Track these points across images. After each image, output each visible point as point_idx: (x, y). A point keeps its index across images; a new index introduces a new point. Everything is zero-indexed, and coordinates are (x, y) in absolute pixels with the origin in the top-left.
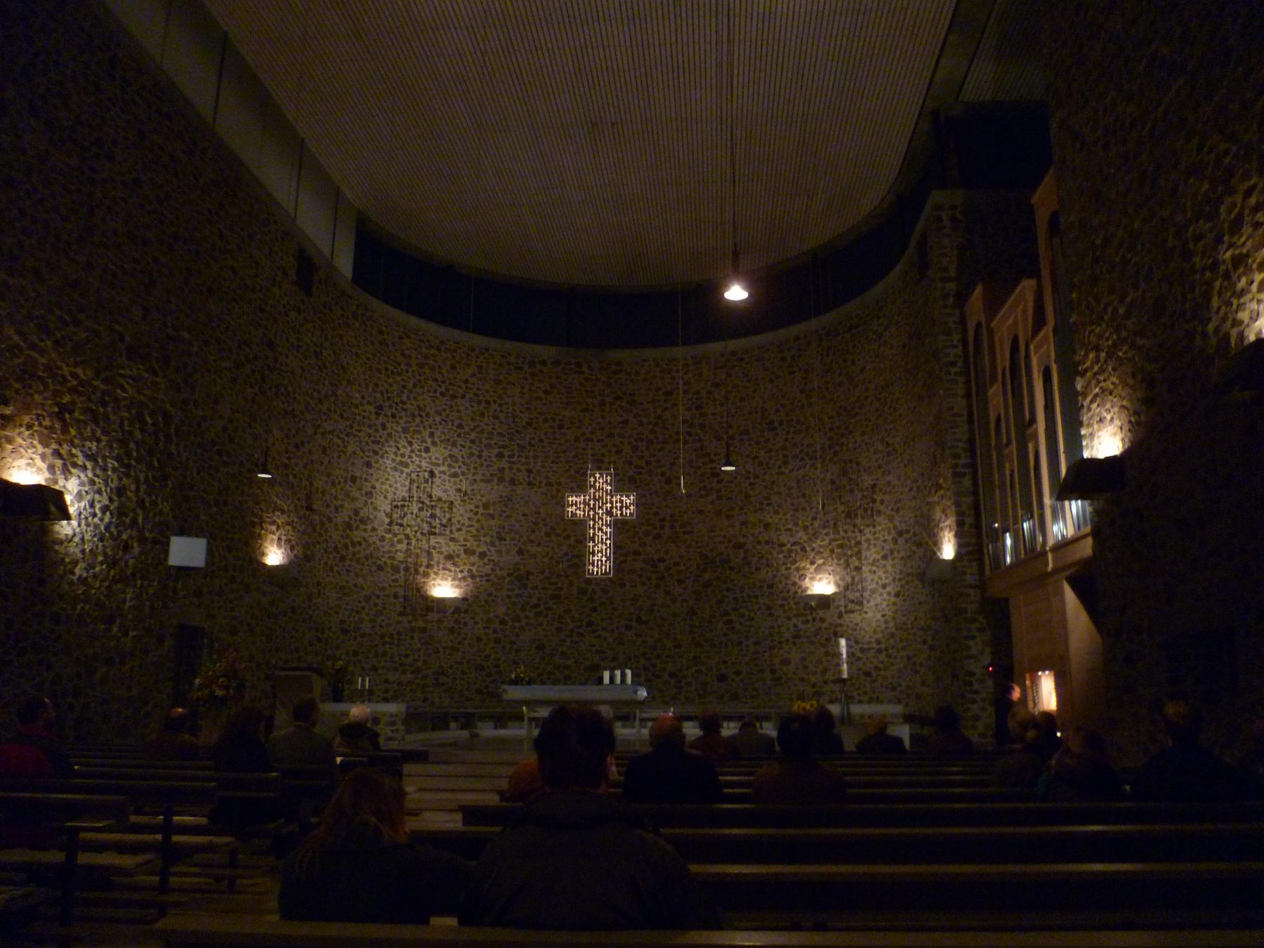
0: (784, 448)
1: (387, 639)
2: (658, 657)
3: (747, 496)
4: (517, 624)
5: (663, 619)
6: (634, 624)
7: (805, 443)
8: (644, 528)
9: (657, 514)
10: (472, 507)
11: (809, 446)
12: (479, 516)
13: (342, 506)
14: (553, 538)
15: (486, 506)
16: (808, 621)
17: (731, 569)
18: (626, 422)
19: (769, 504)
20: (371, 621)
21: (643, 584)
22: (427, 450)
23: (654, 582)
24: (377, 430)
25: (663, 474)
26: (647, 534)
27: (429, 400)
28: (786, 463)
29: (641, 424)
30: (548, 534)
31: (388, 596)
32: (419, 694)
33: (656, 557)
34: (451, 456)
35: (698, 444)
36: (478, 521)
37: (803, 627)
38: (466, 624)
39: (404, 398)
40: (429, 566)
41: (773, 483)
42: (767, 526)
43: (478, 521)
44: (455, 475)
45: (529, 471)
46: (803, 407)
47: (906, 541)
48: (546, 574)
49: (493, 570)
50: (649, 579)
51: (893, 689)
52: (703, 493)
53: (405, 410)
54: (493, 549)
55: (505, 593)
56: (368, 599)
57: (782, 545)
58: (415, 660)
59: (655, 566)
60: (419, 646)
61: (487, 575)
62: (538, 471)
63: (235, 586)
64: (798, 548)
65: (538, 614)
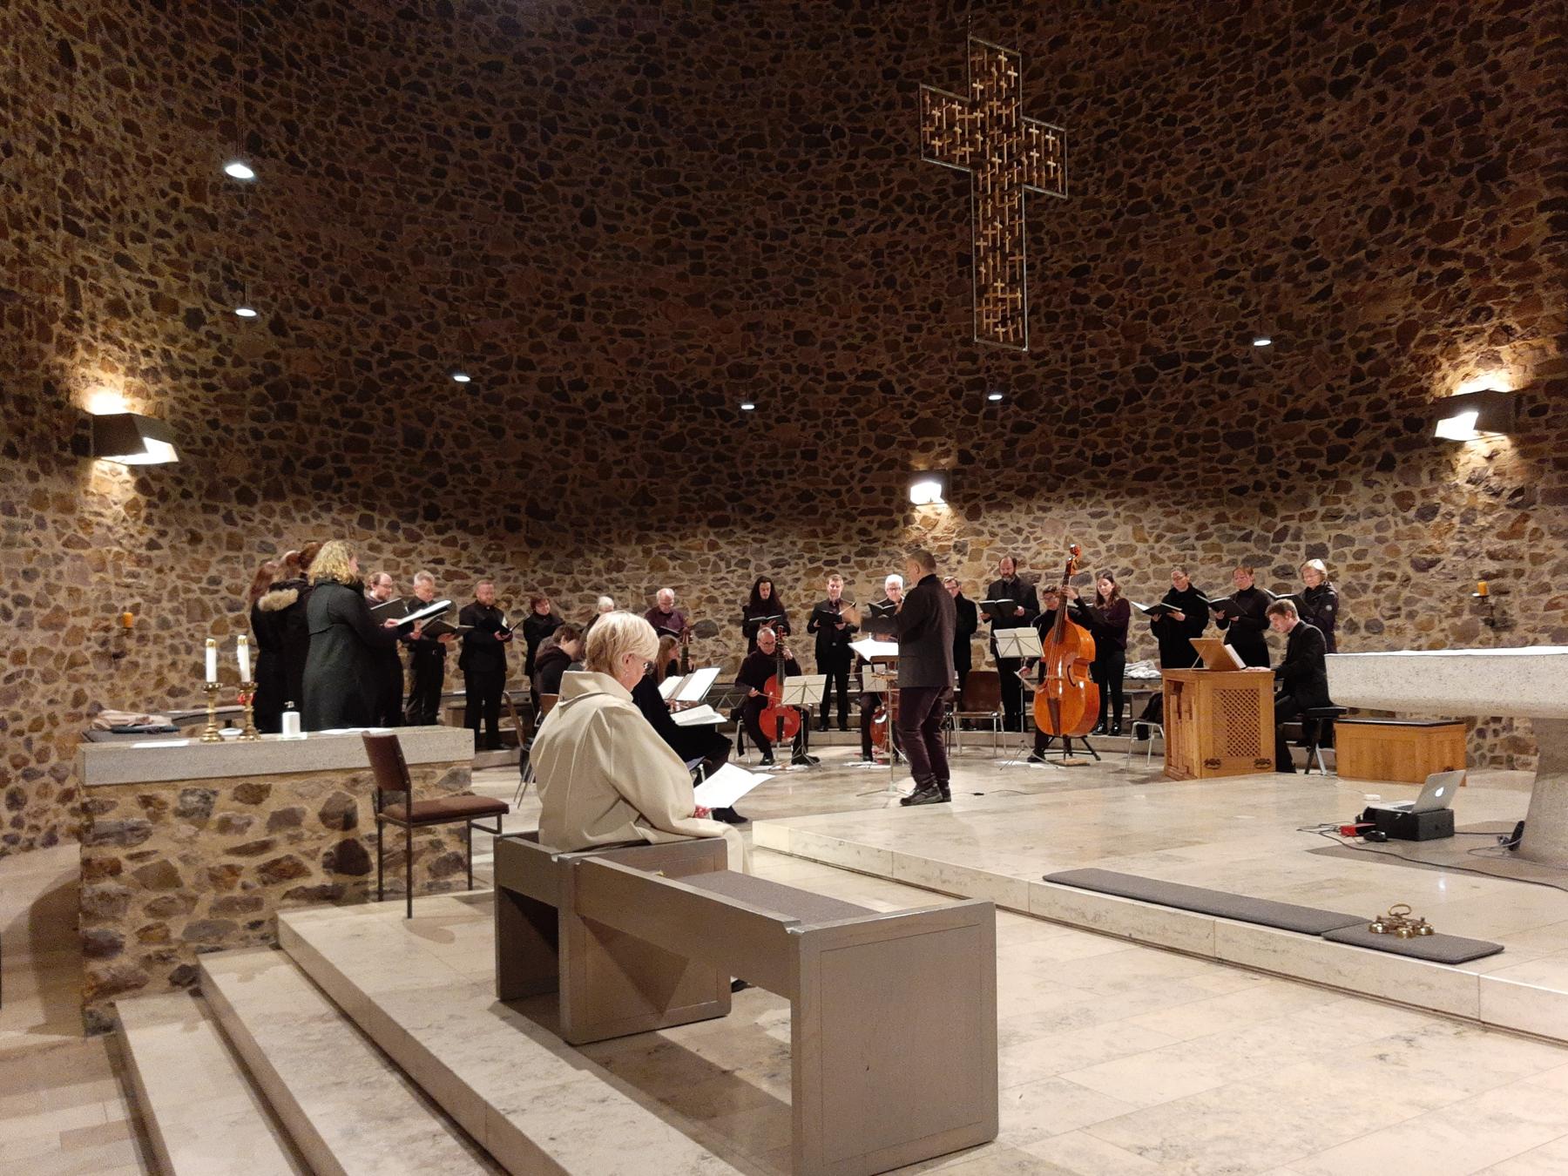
0: (843, 183)
3: (760, 273)
4: (278, 506)
7: (898, 176)
8: (542, 312)
9: (566, 285)
10: (164, 183)
11: (904, 185)
14: (349, 304)
18: (497, 67)
19: (810, 294)
21: (541, 433)
25: (578, 201)
28: (847, 214)
29: (530, 81)
30: (337, 296)
32: (62, 684)
35: (652, 152)
40: (72, 322)
41: (818, 251)
42: (804, 338)
43: (180, 226)
44: (119, 80)
45: (291, 128)
46: (889, 106)
48: (337, 391)
49: (218, 361)
50: (552, 422)
52: (663, 254)
54: (213, 305)
55: (249, 423)
57: (834, 377)
58: (51, 589)
59: (563, 397)
60: (58, 547)
61: (205, 373)
64: (875, 384)
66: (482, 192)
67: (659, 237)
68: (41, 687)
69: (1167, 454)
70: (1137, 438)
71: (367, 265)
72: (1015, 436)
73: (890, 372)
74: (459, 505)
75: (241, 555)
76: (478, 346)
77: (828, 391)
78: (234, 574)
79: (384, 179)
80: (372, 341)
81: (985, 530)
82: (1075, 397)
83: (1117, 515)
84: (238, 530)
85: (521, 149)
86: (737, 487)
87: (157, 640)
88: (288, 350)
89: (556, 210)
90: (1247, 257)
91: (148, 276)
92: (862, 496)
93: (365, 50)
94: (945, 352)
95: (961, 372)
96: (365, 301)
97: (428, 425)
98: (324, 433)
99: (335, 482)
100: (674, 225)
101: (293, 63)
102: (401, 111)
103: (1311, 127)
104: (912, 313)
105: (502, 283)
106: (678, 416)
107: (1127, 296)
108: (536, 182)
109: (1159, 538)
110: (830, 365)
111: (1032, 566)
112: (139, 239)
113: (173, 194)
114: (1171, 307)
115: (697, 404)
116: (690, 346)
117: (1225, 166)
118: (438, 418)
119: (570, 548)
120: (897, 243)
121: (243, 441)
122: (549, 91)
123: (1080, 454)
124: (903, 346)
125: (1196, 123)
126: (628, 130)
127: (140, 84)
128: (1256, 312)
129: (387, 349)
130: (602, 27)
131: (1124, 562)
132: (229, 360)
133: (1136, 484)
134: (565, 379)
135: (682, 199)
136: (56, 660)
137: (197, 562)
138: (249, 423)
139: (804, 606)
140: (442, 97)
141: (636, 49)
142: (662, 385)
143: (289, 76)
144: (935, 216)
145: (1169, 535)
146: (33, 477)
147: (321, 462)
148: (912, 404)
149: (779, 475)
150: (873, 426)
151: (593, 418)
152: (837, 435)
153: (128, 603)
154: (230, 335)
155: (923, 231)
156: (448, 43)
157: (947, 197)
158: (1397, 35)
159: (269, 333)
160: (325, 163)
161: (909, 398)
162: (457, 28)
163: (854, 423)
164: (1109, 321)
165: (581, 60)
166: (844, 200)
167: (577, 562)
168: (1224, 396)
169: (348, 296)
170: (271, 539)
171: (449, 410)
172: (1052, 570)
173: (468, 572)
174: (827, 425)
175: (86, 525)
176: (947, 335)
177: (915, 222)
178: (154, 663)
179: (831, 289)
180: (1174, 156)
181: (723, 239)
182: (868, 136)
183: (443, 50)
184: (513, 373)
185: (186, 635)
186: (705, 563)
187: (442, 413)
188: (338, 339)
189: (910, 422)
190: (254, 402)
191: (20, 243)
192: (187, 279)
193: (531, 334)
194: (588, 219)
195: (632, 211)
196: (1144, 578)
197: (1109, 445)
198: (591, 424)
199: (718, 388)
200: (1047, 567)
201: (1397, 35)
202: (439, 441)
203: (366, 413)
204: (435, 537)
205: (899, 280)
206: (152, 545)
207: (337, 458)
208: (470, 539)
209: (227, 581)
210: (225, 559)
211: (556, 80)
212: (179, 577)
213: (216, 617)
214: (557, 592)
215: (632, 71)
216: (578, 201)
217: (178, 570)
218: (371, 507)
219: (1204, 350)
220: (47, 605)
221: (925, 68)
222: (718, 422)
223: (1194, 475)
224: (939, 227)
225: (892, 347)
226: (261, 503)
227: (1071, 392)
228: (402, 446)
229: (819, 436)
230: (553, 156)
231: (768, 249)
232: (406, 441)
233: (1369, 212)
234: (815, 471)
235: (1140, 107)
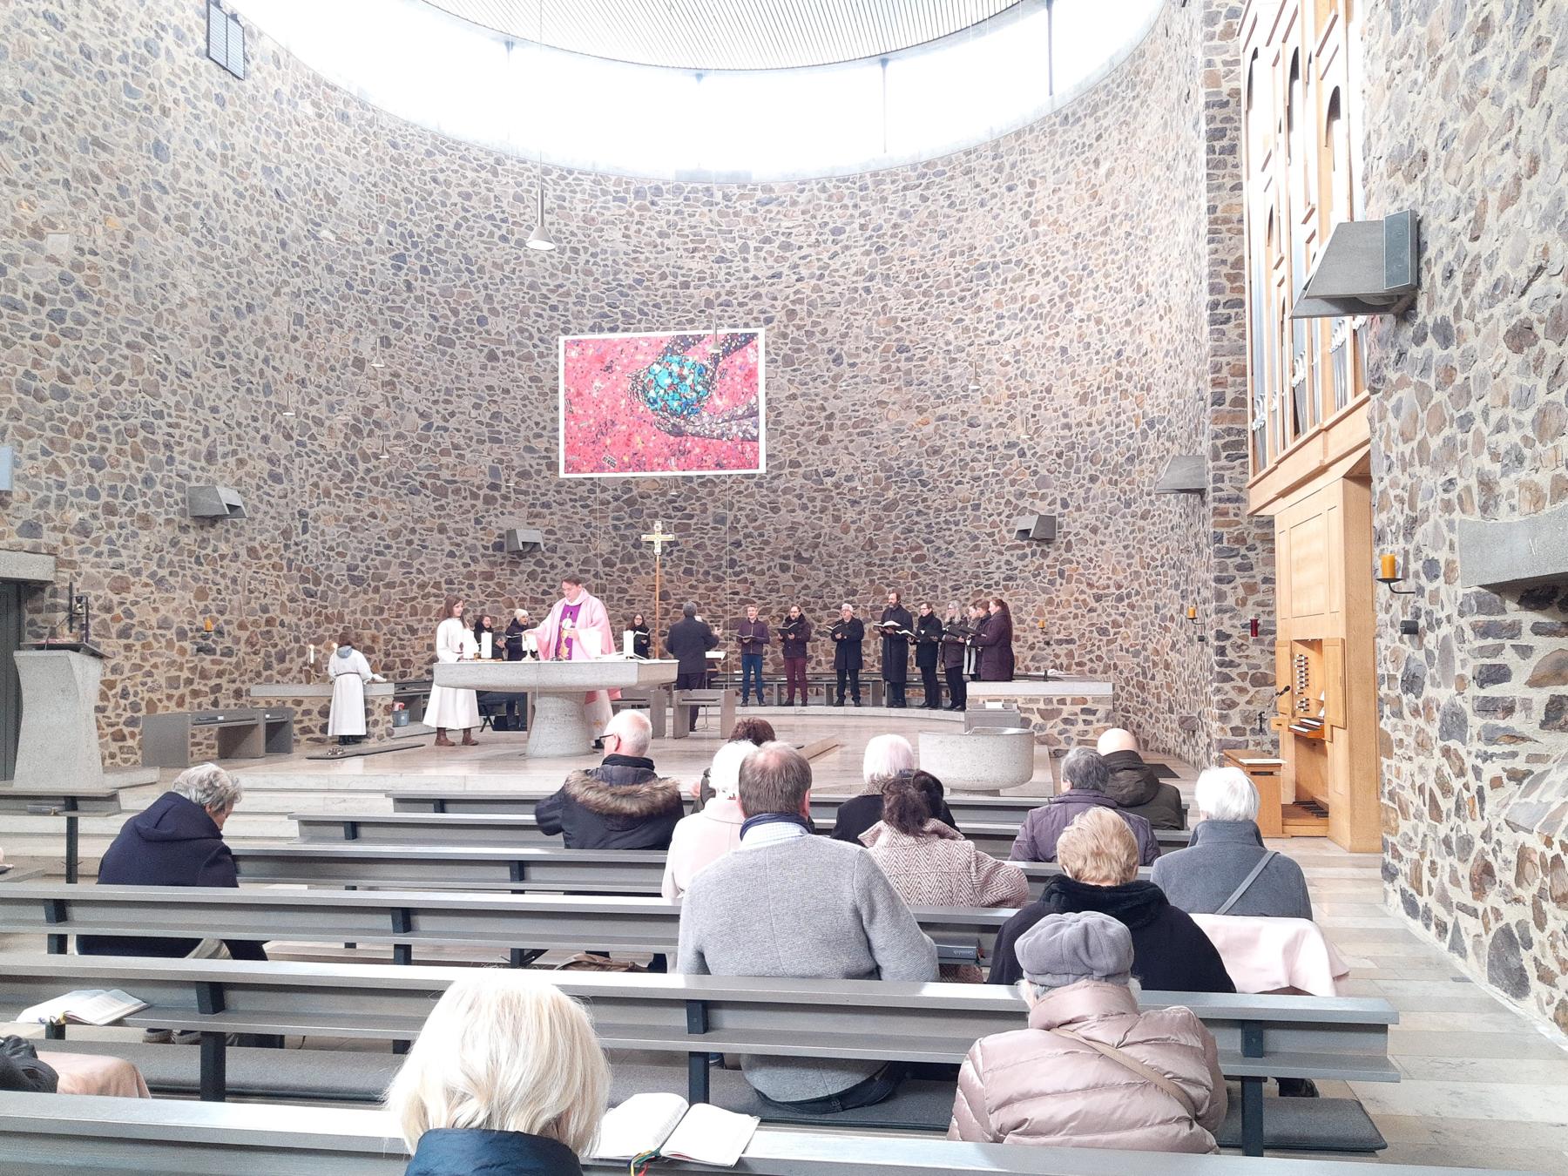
0: (998, 303)
1: (429, 589)
2: (825, 607)
4: (629, 567)
5: (830, 555)
6: (791, 562)
8: (806, 429)
11: (1033, 299)
13: (340, 403)
16: (1025, 556)
17: (924, 484)
20: (402, 565)
21: (804, 507)
22: (482, 321)
23: (818, 503)
24: (395, 292)
25: (831, 351)
26: (808, 437)
27: (482, 246)
31: (431, 530)
34: (521, 330)
37: (1019, 564)
38: (553, 567)
39: (441, 244)
44: (529, 358)
49: (590, 491)
50: (813, 499)
51: (1136, 654)
53: (446, 263)
55: (611, 522)
56: (396, 534)
60: (482, 597)
63: (116, 520)
64: (1014, 451)
74: (749, 558)
93: (692, 290)
101: (641, 312)
105: (780, 414)
112: (540, 436)
122: (813, 282)
130: (848, 229)
133: (1141, 523)
138: (611, 522)
140: (741, 305)
141: (871, 237)
143: (640, 321)
146: (466, 565)
149: (957, 524)
150: (1013, 482)
156: (746, 270)
165: (835, 255)
171: (744, 500)
175: (501, 585)
176: (1055, 411)
177: (1038, 326)
181: (924, 359)
183: (742, 274)
186: (909, 588)
193: (799, 444)
194: (838, 360)
196: (1144, 599)
197: (1132, 491)
198: (837, 499)
202: (738, 521)
206: (545, 593)
208: (756, 578)
214: (813, 611)
215: (867, 253)
218: (692, 563)
229: (982, 493)
230: (815, 324)
231: (954, 360)
232: (716, 521)
234: (978, 518)
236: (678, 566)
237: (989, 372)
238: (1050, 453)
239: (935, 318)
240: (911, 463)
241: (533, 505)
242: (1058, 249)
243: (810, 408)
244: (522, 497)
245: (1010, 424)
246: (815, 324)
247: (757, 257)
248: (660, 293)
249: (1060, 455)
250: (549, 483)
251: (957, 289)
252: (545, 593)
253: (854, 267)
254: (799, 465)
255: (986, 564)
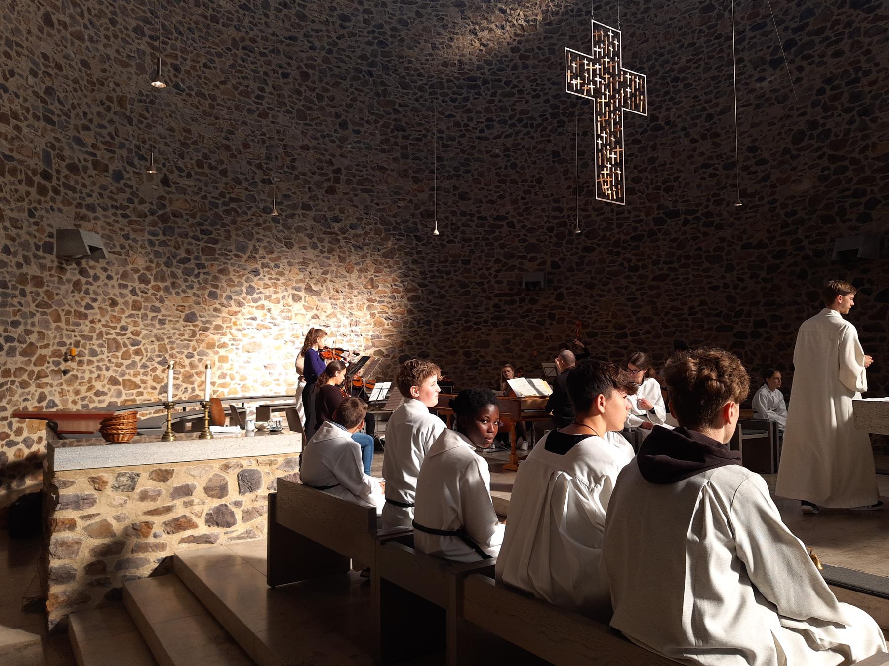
0: (488, 110)
4: (162, 285)
6: (302, 294)
7: (519, 107)
11: (524, 112)
12: (110, 115)
14: (206, 170)
15: (121, 101)
16: (513, 302)
17: (418, 238)
18: (293, 38)
19: (468, 172)
25: (338, 116)
26: (318, 185)
30: (200, 164)
32: (32, 388)
33: (329, 215)
36: (111, 122)
38: (96, 278)
43: (111, 122)
45: (177, 68)
46: (515, 67)
47: (686, 222)
48: (198, 219)
49: (130, 201)
52: (384, 146)
54: (129, 168)
60: (33, 307)
62: (187, 72)
64: (504, 223)
65: (187, 273)
66: (284, 109)
67: (384, 137)
68: (20, 391)
69: (672, 266)
70: (655, 257)
71: (218, 148)
72: (584, 254)
73: (513, 216)
75: (140, 313)
76: (279, 196)
77: (477, 226)
78: (136, 324)
79: (228, 99)
80: (219, 192)
81: (566, 306)
82: (619, 233)
83: (643, 300)
84: (138, 299)
85: (307, 86)
86: (425, 279)
87: (90, 362)
88: (171, 196)
89: (325, 121)
90: (719, 157)
91: (91, 150)
92: (496, 286)
93: (220, 26)
94: (545, 206)
95: (554, 217)
96: (216, 168)
97: (251, 240)
98: (190, 244)
99: (196, 272)
100: (392, 131)
102: (240, 62)
103: (758, 85)
104: (526, 184)
105: (294, 160)
106: (392, 239)
107: (649, 177)
108: (315, 104)
109: (667, 314)
110: (478, 212)
111: (593, 328)
112: (86, 128)
113: (108, 103)
114: (675, 184)
115: (403, 232)
116: (399, 199)
117: (707, 106)
118: (256, 236)
119: (329, 312)
120: (519, 144)
121: (142, 247)
122: (323, 53)
123: (622, 265)
124: (520, 202)
125: (690, 81)
126: (367, 77)
127: (91, 39)
128: (726, 188)
129: (228, 196)
130: (354, 19)
131: (647, 327)
132: (136, 200)
133: (654, 283)
134: (329, 215)
135: (395, 116)
136: (29, 375)
137: (115, 317)
138: (147, 237)
139: (462, 348)
140: (263, 55)
141: (373, 31)
142: (384, 222)
144: (539, 130)
145: (673, 312)
147: (189, 260)
148: (525, 235)
149: (448, 273)
150: (502, 246)
151: (345, 238)
152: (482, 251)
153: (72, 341)
154: (138, 186)
155: (533, 138)
157: (547, 119)
158: (809, 34)
159: (161, 185)
160: (195, 89)
161: (524, 231)
162: (272, 17)
163: (492, 244)
164: (639, 191)
166: (488, 120)
167: (334, 320)
168: (705, 234)
169: (206, 166)
170: (157, 304)
172: (604, 330)
173: (271, 325)
174: (476, 245)
176: (546, 196)
177: (528, 133)
178: (87, 376)
179: (480, 169)
180: (677, 99)
182: (502, 84)
183: (263, 27)
184: (300, 211)
185: (106, 359)
187: (258, 233)
188: (200, 189)
189: (524, 245)
190: (150, 225)
191: (18, 128)
192: (114, 153)
194: (343, 125)
195: (368, 122)
197: (638, 260)
199: (415, 223)
200: (602, 328)
201: (809, 34)
203: (215, 233)
204: (253, 304)
205: (519, 165)
207: (197, 258)
209: (131, 328)
210: (131, 316)
211: (328, 47)
212: (103, 326)
213: (124, 349)
215: (370, 44)
216: (338, 116)
217: (103, 322)
219: (694, 207)
220: (25, 342)
221: (535, 47)
222: (415, 242)
223: (688, 279)
224: (542, 136)
225: (514, 202)
226: (152, 283)
227: (616, 230)
228: (234, 252)
229: (472, 251)
230: (326, 90)
233: (793, 132)
235: (658, 71)
236: (204, 288)
237: (479, 160)
238: (542, 227)
239: (430, 109)
240: (407, 221)
241: (79, 205)
242: (549, 80)
243: (320, 161)
244: (70, 193)
245: (499, 201)
246: (326, 90)
247: (276, 17)
248: (194, 18)
249: (551, 229)
250: (94, 184)
251: (450, 92)
252: (89, 307)
253: (359, 52)
254: (310, 209)
255: (475, 306)
